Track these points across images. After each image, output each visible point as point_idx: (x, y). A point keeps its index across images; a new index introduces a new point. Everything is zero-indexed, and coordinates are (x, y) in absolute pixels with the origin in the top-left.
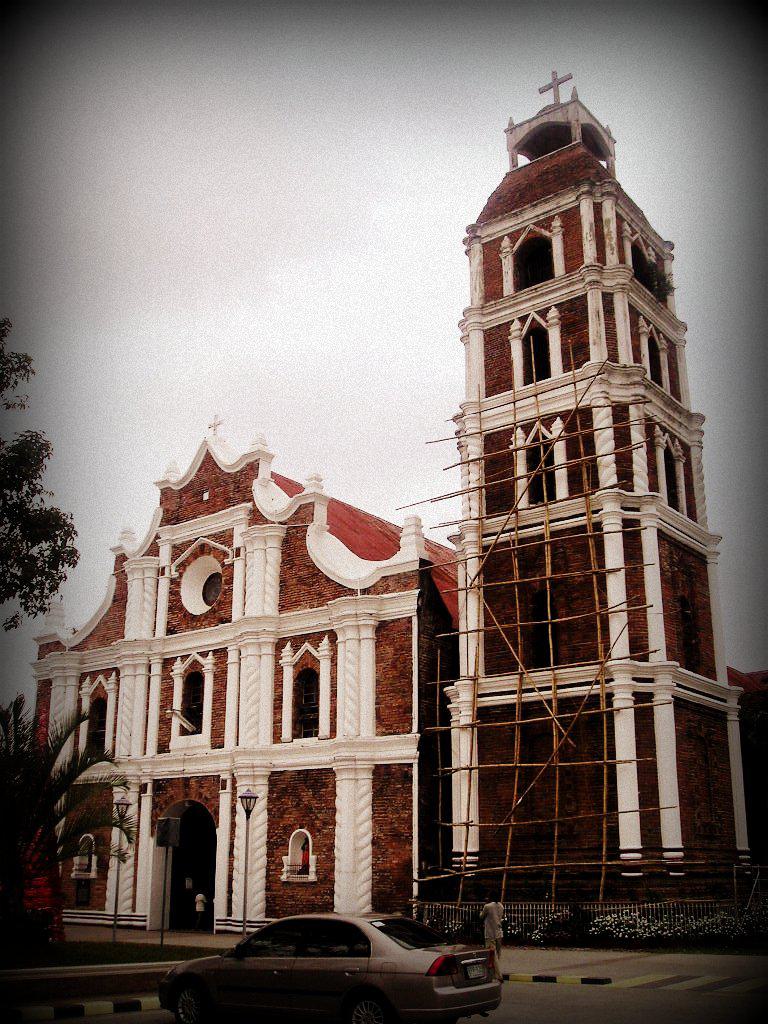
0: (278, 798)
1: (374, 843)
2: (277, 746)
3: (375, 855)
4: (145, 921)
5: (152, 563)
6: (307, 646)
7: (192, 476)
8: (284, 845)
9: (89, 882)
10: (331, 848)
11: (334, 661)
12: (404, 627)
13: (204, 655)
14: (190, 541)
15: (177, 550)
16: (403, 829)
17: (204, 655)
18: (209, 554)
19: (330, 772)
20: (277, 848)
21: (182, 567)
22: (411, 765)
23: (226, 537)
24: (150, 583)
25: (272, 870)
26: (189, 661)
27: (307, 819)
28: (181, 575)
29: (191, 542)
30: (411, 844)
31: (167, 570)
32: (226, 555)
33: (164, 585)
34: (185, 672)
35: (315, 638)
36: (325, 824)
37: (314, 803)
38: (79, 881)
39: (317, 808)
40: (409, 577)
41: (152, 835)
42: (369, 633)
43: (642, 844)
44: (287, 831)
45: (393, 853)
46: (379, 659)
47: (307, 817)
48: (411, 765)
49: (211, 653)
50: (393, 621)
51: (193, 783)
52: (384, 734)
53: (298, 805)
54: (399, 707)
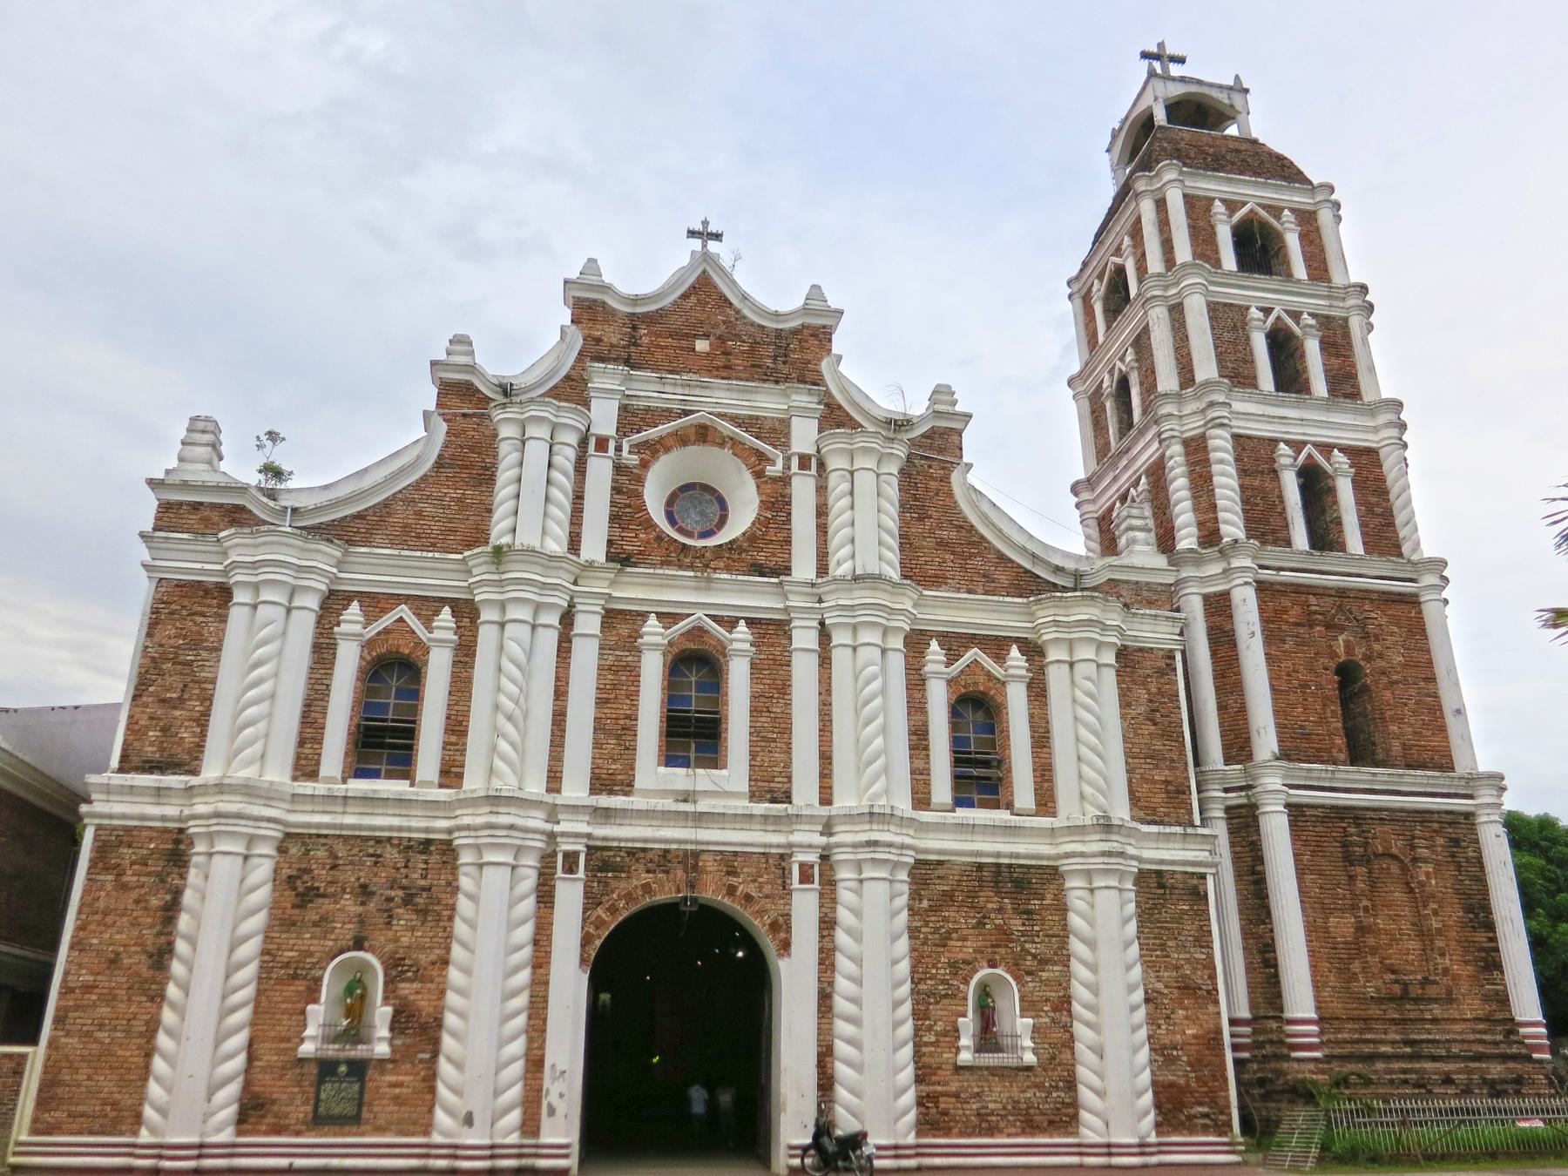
0: (933, 909)
1: (1147, 1000)
2: (925, 816)
3: (1152, 1021)
4: (566, 1156)
5: (569, 417)
6: (974, 653)
7: (667, 302)
8: (954, 996)
9: (359, 1068)
10: (1064, 1003)
11: (1038, 691)
12: (1162, 664)
13: (731, 624)
14: (669, 410)
15: (630, 418)
16: (1200, 978)
17: (731, 624)
18: (722, 445)
19: (1052, 874)
20: (937, 1003)
21: (651, 450)
22: (1203, 877)
23: (778, 432)
24: (566, 457)
25: (927, 1044)
26: (683, 626)
27: (1003, 951)
28: (645, 465)
29: (668, 415)
30: (1216, 1002)
31: (612, 445)
32: (762, 457)
33: (600, 471)
34: (670, 644)
35: (997, 646)
36: (1043, 962)
37: (1016, 924)
38: (326, 1068)
39: (1024, 934)
40: (1155, 592)
41: (583, 961)
42: (1109, 657)
43: (1251, 1012)
44: (962, 969)
45: (1186, 1018)
46: (1125, 703)
47: (999, 946)
48: (1203, 877)
49: (742, 622)
50: (1141, 650)
51: (709, 864)
52: (1144, 822)
53: (981, 924)
54: (1167, 782)
